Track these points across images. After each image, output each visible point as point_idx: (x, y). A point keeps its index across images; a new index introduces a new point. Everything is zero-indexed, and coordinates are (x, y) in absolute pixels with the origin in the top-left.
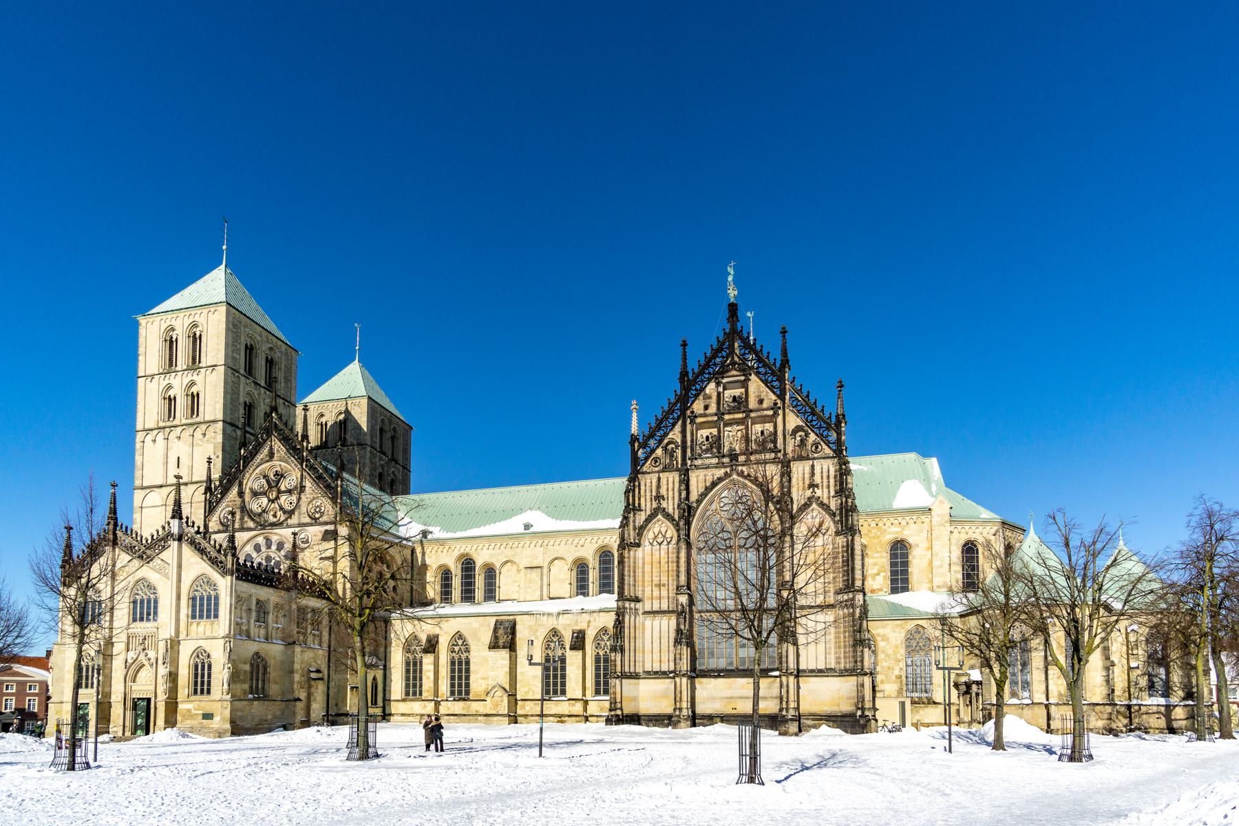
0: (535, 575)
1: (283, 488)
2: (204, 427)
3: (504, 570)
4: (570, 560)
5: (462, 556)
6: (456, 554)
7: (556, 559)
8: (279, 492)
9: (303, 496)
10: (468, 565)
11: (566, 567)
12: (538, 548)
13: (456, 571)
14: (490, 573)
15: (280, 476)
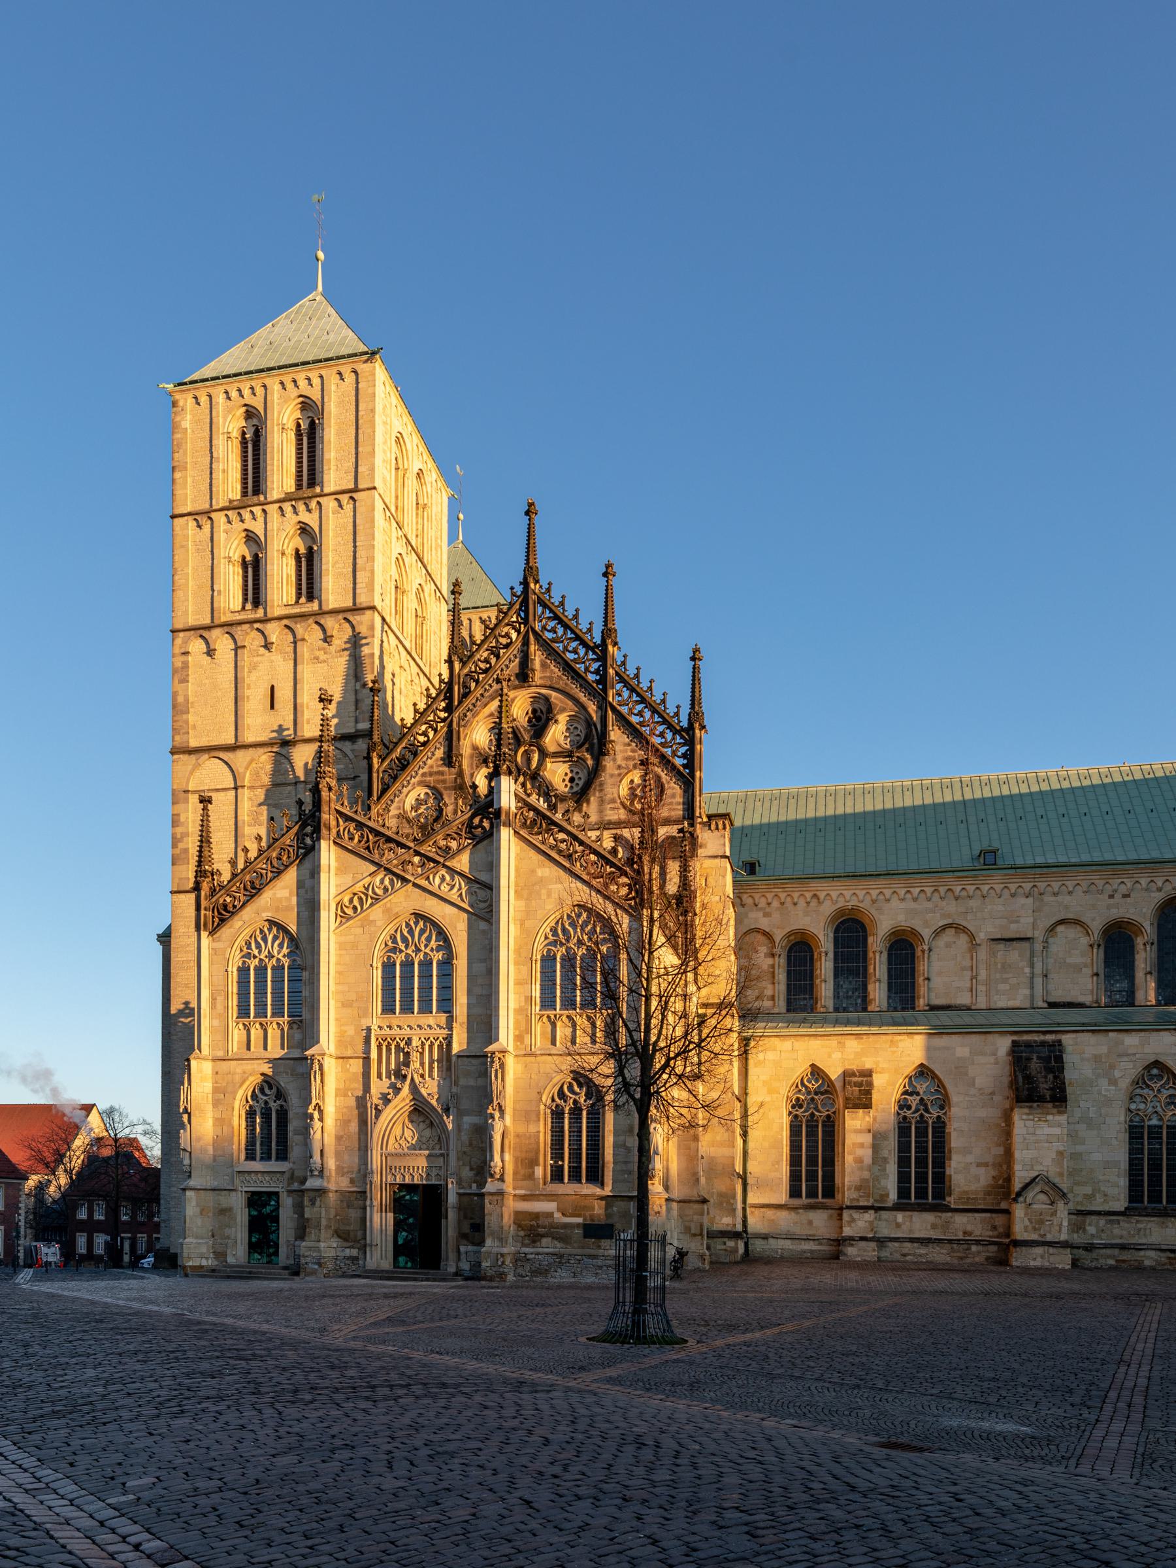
0: (1014, 955)
1: (552, 749)
2: (330, 622)
3: (941, 942)
4: (1097, 926)
5: (841, 912)
6: (828, 909)
7: (1062, 922)
8: (544, 754)
9: (608, 763)
10: (851, 930)
11: (1085, 941)
12: (1023, 900)
13: (825, 943)
14: (903, 949)
15: (541, 718)
